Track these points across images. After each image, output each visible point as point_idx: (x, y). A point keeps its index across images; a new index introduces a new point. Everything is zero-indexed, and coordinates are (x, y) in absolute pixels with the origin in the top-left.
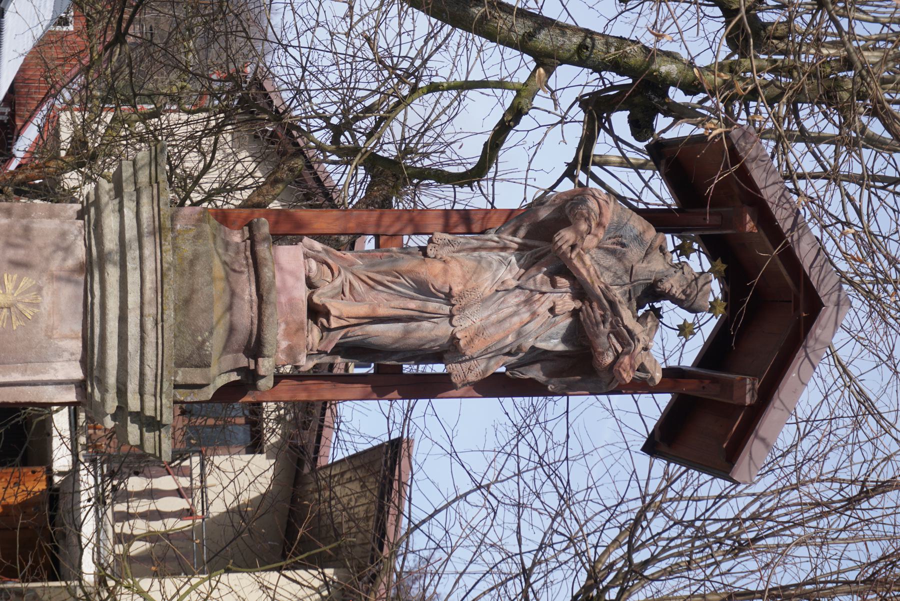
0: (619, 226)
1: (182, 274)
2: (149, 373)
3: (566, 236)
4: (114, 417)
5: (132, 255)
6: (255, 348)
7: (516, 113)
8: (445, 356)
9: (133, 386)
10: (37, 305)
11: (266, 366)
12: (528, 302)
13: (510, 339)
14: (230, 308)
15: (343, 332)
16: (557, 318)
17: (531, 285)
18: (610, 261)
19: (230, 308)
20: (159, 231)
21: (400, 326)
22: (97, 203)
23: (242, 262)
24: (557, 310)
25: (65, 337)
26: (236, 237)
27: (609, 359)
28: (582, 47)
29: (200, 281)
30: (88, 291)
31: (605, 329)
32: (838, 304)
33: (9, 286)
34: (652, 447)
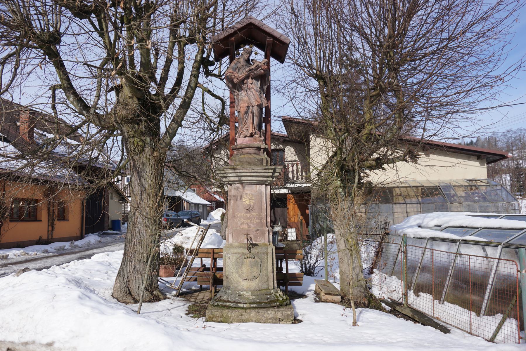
0: (233, 69)
1: (243, 164)
2: (264, 171)
3: (235, 80)
4: (273, 178)
5: (239, 174)
6: (259, 149)
7: (209, 92)
9: (267, 174)
11: (263, 147)
12: (250, 89)
14: (250, 154)
18: (241, 71)
19: (250, 154)
20: (234, 169)
21: (255, 118)
22: (228, 182)
23: (241, 151)
26: (235, 152)
27: (262, 71)
28: (194, 77)
29: (245, 160)
30: (246, 184)
31: (256, 72)
32: (251, 19)
34: (282, 62)
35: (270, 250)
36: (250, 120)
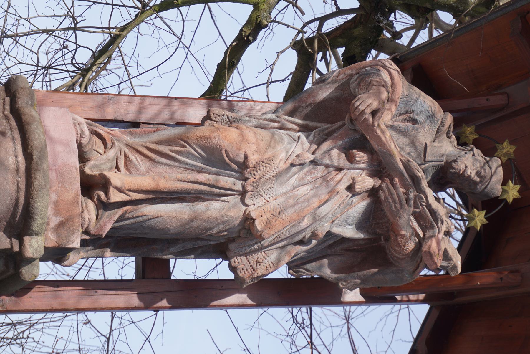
8: (232, 246)
11: (34, 246)
13: (306, 222)
15: (120, 212)
16: (355, 199)
17: (327, 161)
18: (405, 141)
24: (358, 187)
27: (411, 246)
36: (170, 178)
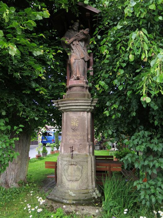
6: (83, 87)
10: (75, 119)
25: (80, 115)
33: (73, 122)
35: (89, 159)
